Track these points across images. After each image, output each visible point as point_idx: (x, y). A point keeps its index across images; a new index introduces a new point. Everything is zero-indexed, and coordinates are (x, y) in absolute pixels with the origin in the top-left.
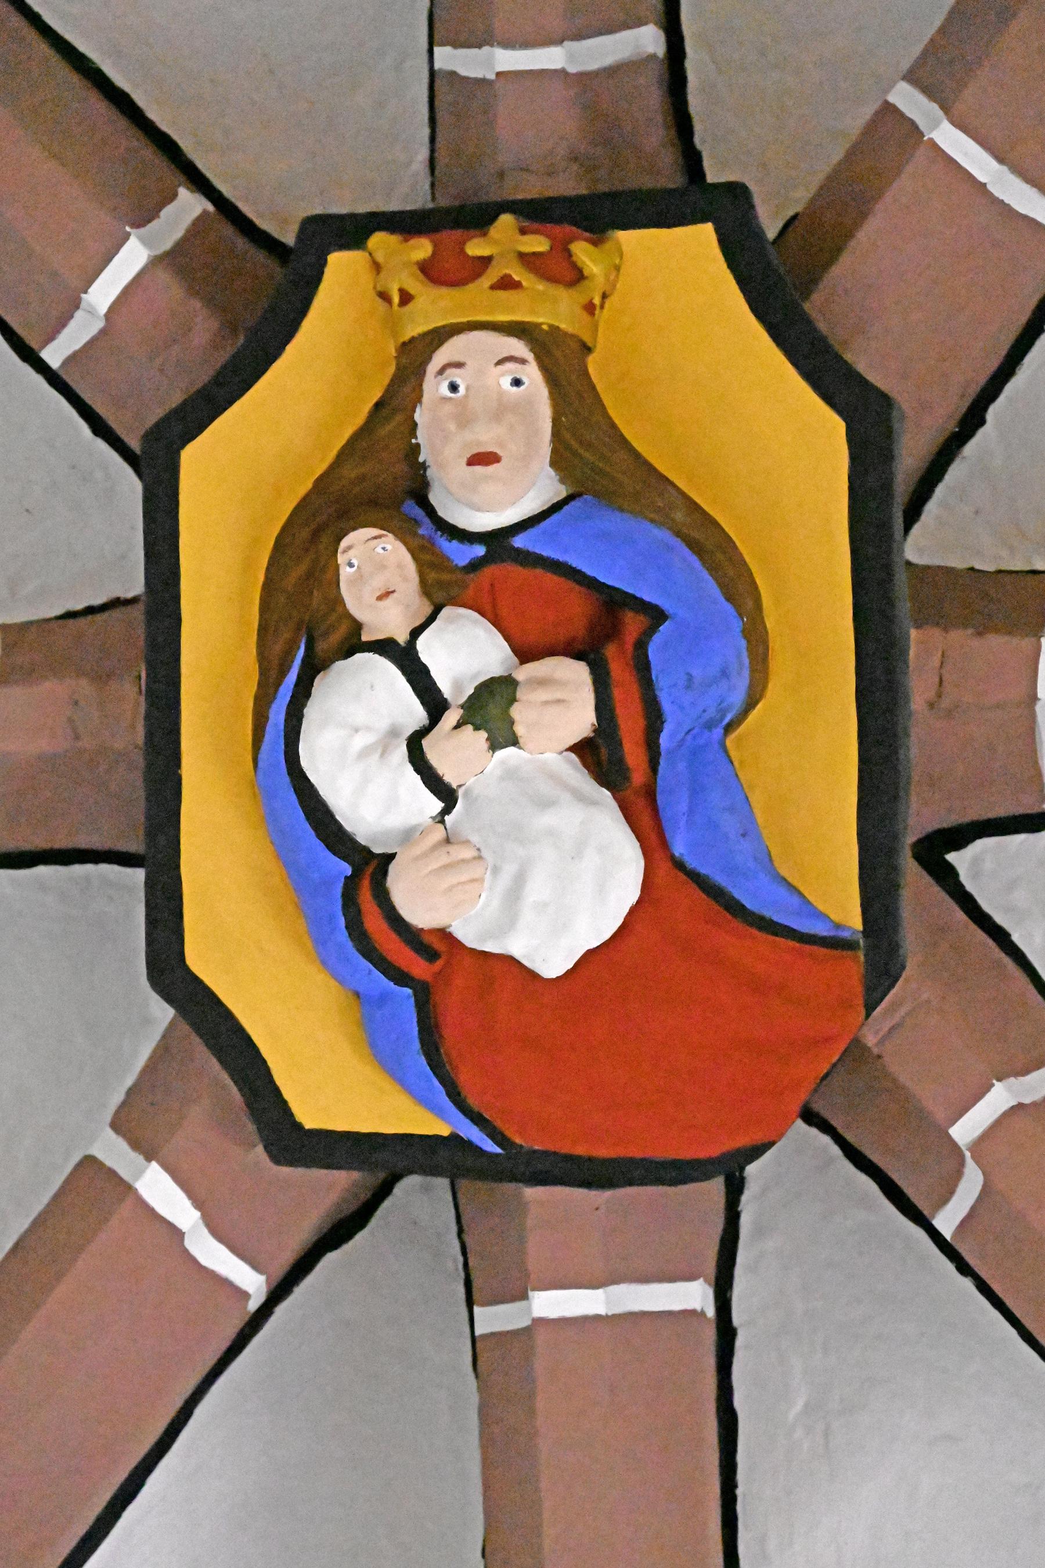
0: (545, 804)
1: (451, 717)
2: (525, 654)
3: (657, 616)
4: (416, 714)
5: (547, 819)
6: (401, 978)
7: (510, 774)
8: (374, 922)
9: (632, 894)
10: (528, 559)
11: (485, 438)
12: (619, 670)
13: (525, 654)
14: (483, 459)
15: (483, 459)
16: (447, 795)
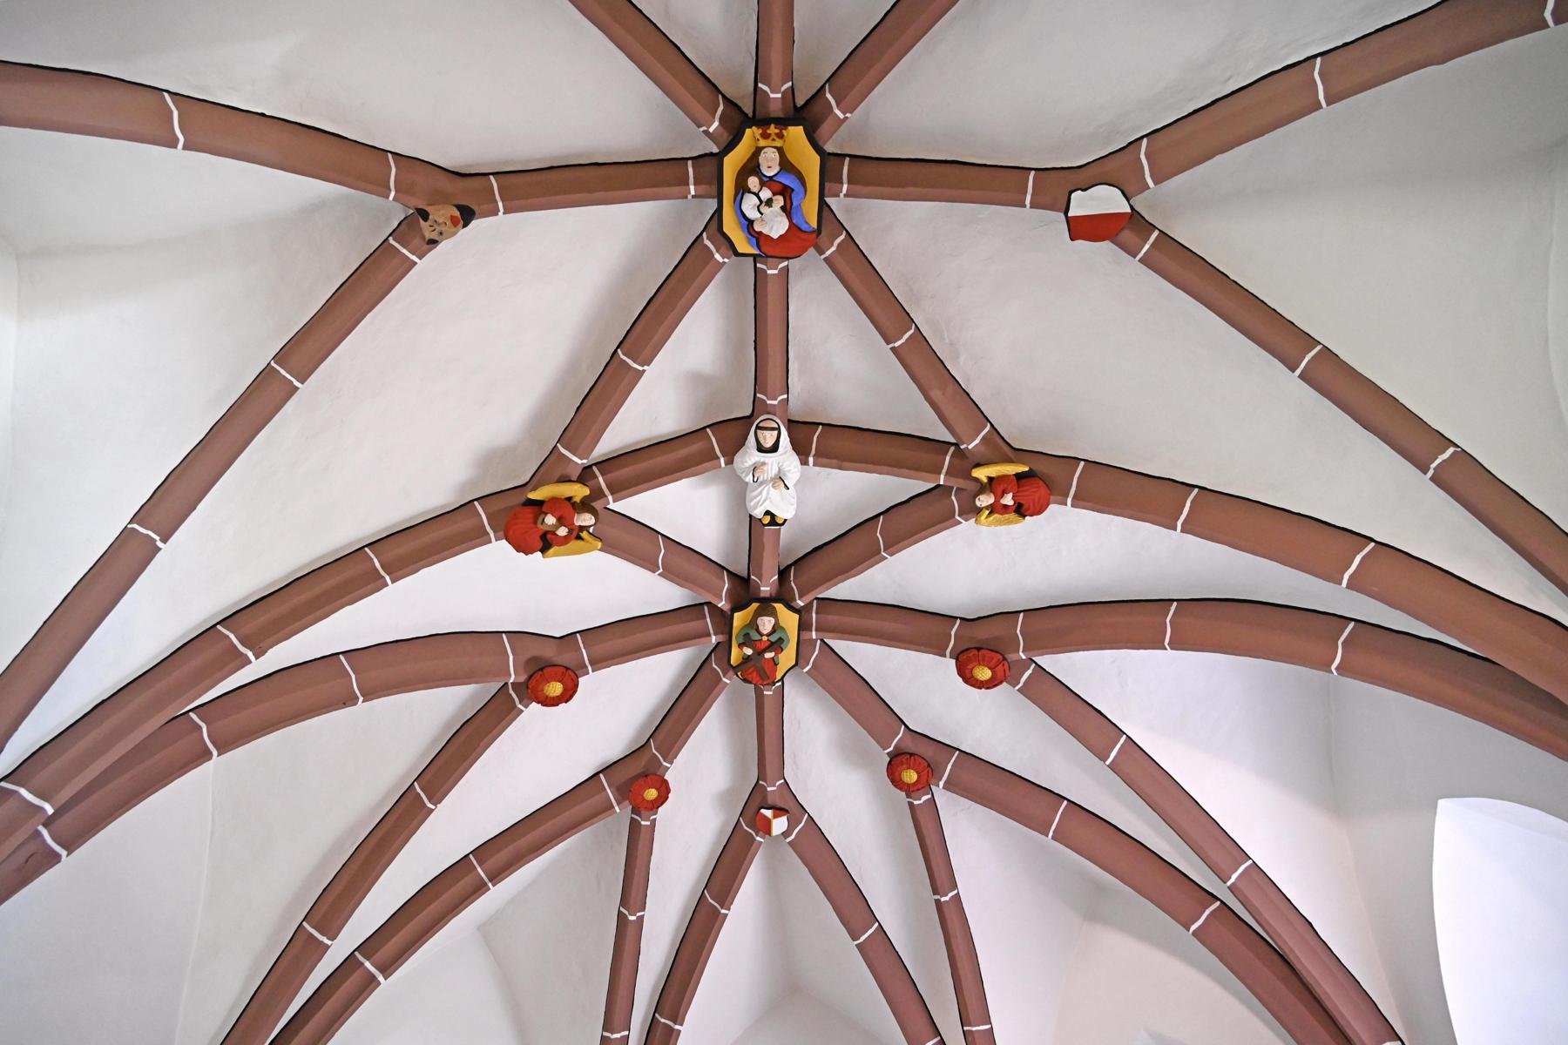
0: (776, 216)
1: (763, 204)
2: (774, 194)
3: (793, 190)
4: (758, 202)
5: (776, 219)
6: (754, 237)
7: (771, 211)
8: (751, 231)
9: (787, 227)
10: (775, 181)
11: (770, 164)
12: (787, 198)
13: (774, 194)
14: (769, 167)
15: (769, 167)
16: (762, 214)
